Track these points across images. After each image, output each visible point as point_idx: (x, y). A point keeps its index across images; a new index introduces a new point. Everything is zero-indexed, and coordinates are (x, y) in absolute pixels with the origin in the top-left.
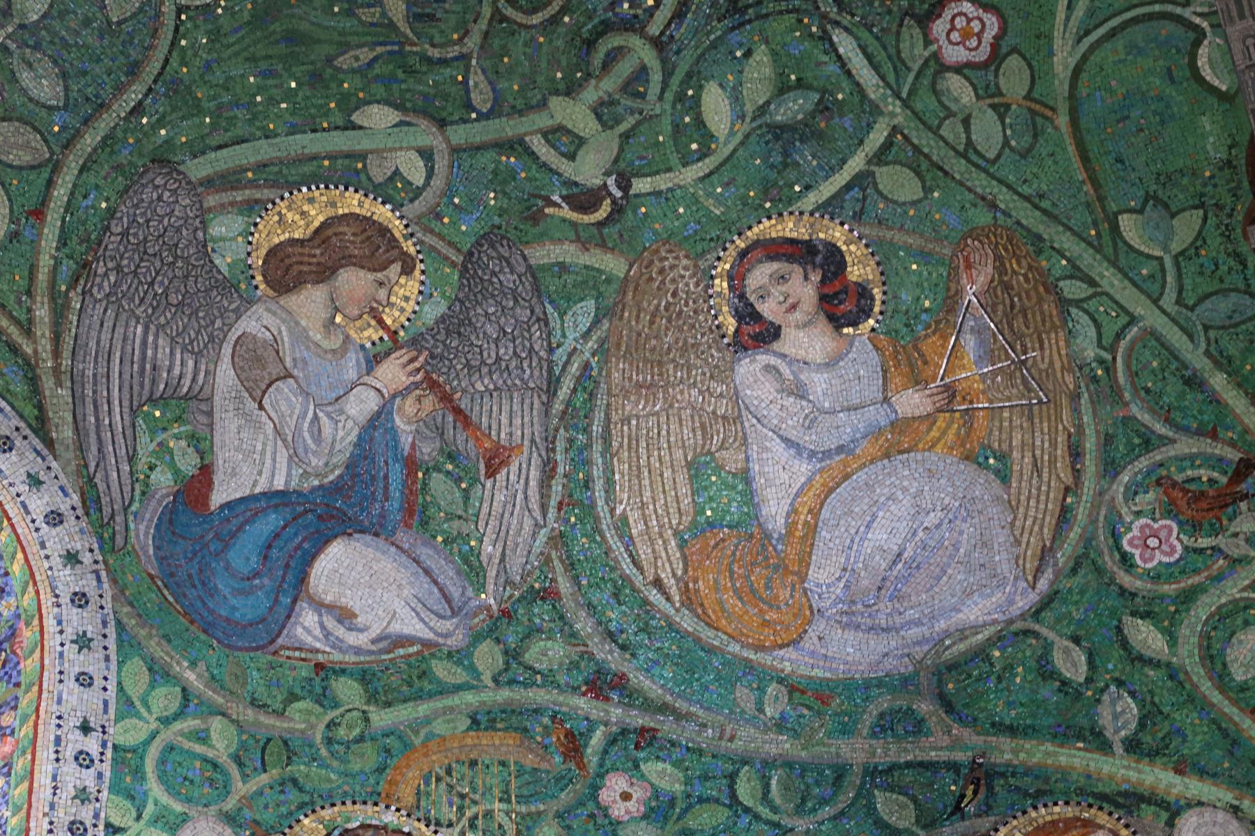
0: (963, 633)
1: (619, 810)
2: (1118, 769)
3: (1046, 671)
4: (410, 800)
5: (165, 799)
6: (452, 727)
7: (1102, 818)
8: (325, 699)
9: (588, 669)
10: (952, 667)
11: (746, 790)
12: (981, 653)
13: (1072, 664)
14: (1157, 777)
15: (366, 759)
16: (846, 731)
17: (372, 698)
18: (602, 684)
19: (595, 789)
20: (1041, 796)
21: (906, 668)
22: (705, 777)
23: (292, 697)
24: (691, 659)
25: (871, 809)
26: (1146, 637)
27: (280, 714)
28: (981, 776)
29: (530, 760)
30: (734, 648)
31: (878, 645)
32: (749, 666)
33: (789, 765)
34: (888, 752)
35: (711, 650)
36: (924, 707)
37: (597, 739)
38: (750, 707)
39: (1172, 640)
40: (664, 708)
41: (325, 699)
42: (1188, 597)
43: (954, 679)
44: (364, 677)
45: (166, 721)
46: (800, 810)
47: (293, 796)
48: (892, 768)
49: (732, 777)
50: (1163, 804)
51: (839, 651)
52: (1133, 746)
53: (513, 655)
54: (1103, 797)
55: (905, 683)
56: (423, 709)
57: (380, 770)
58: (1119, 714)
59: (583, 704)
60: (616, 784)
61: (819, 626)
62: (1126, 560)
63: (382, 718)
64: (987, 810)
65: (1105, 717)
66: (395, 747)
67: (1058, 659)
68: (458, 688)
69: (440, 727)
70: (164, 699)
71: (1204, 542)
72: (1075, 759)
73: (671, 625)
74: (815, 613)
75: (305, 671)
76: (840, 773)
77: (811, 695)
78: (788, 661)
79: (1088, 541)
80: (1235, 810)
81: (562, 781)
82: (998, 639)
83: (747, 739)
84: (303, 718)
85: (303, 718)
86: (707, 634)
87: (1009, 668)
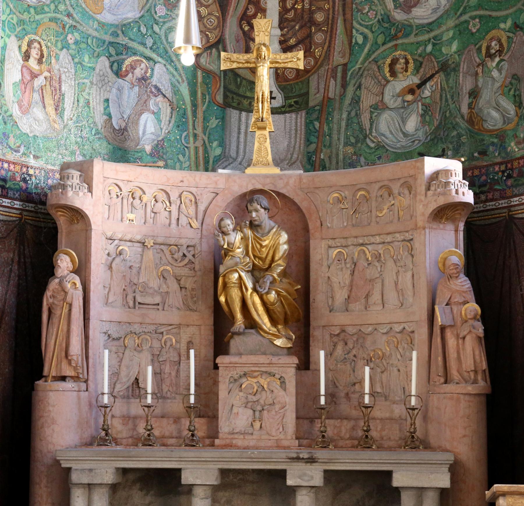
0: (128, 18)
1: (70, 41)
2: (148, 53)
3: (139, 31)
4: (40, 35)
5: (8, 32)
6: (46, 20)
7: (144, 61)
8: (29, 12)
9: (67, 12)
10: (125, 25)
11: (89, 41)
12: (129, 23)
13: (143, 30)
14: (154, 56)
15: (34, 26)
16: (106, 33)
17: (36, 13)
18: (69, 15)
19: (67, 36)
20: (135, 54)
21: (116, 22)
22: (83, 38)
23: (24, 12)
24: (84, 13)
25: (108, 49)
26: (156, 28)
27: (23, 14)
28: (127, 48)
29: (57, 29)
30: (90, 12)
31: (114, 17)
32: (93, 17)
33: (97, 38)
34: (112, 40)
35: (87, 12)
36: (119, 32)
37: (67, 26)
38: (92, 25)
39: (160, 29)
40: (78, 22)
41: (29, 12)
42: (164, 23)
43: (124, 28)
44: (35, 8)
45: (8, 15)
46: (97, 48)
47: (24, 32)
48: (113, 43)
49: (88, 38)
50: (154, 61)
51: (107, 17)
52: (151, 48)
53: (56, 7)
54: (145, 57)
55: (117, 26)
56: (43, 16)
57: (36, 28)
58: (149, 42)
59: (66, 19)
60: (70, 36)
61: (104, 11)
62: (156, 12)
63: (37, 17)
64: (127, 54)
65: (147, 42)
66: (38, 23)
67: (142, 29)
68: (48, 12)
69: (45, 20)
70: (8, 11)
71: (169, 13)
72: (141, 48)
73: (81, 6)
74: (104, 9)
75: (26, 6)
76: (104, 42)
77: (102, 25)
78: (98, 17)
79: (150, 7)
80: (165, 65)
81: (62, 34)
82: (132, 22)
83: (91, 32)
84: (26, 16)
85: (26, 16)
86: (88, 10)
87: (133, 28)
